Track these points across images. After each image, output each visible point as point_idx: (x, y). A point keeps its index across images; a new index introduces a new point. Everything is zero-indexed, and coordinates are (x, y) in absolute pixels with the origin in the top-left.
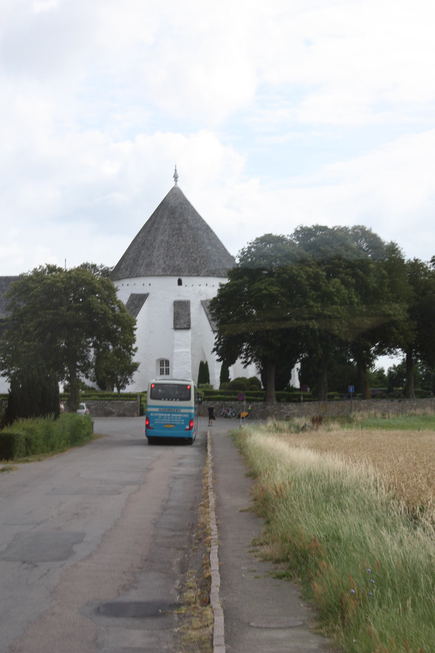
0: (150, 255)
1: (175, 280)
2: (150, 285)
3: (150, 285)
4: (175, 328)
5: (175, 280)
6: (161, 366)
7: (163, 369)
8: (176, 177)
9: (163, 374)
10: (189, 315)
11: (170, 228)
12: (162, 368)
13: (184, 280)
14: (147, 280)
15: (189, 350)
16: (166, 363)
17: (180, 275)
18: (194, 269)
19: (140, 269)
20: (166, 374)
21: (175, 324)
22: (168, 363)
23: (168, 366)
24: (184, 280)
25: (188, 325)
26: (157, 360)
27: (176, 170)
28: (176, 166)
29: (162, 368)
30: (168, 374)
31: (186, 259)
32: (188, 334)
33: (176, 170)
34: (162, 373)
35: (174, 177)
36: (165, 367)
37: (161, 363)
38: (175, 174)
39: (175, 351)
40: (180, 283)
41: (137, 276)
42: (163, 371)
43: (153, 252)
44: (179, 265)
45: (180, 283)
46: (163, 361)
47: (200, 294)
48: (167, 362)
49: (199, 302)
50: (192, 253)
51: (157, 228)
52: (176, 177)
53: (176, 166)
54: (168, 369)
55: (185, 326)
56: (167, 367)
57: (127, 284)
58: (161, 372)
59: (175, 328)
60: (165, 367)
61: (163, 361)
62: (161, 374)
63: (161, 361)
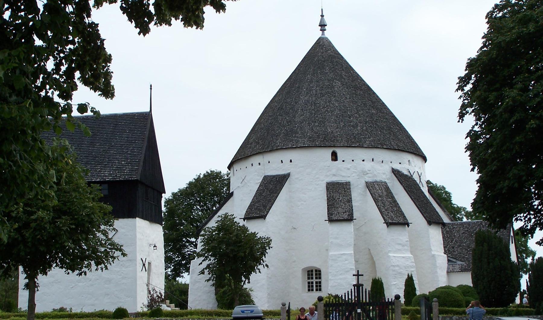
0: (290, 121)
1: (328, 153)
2: (291, 161)
3: (291, 161)
4: (331, 220)
5: (328, 153)
6: (309, 278)
7: (312, 283)
8: (323, 26)
9: (313, 290)
10: (350, 201)
11: (317, 87)
12: (310, 281)
13: (341, 153)
14: (286, 155)
15: (353, 252)
16: (316, 274)
17: (334, 146)
18: (355, 137)
19: (277, 140)
20: (317, 290)
21: (330, 214)
22: (320, 274)
23: (320, 278)
24: (341, 153)
25: (349, 215)
26: (303, 270)
27: (322, 16)
28: (322, 9)
29: (310, 281)
30: (320, 290)
31: (342, 124)
32: (347, 229)
33: (322, 16)
34: (310, 289)
36: (314, 281)
37: (308, 275)
39: (330, 253)
40: (334, 157)
41: (271, 151)
42: (312, 286)
43: (294, 117)
44: (332, 132)
45: (334, 157)
46: (312, 271)
47: (365, 173)
48: (318, 273)
49: (364, 184)
50: (350, 118)
51: (299, 87)
52: (323, 26)
53: (322, 9)
54: (320, 282)
55: (346, 217)
56: (318, 280)
57: (258, 164)
58: (309, 286)
59: (331, 220)
60: (314, 281)
61: (312, 271)
62: (309, 290)
63: (308, 271)
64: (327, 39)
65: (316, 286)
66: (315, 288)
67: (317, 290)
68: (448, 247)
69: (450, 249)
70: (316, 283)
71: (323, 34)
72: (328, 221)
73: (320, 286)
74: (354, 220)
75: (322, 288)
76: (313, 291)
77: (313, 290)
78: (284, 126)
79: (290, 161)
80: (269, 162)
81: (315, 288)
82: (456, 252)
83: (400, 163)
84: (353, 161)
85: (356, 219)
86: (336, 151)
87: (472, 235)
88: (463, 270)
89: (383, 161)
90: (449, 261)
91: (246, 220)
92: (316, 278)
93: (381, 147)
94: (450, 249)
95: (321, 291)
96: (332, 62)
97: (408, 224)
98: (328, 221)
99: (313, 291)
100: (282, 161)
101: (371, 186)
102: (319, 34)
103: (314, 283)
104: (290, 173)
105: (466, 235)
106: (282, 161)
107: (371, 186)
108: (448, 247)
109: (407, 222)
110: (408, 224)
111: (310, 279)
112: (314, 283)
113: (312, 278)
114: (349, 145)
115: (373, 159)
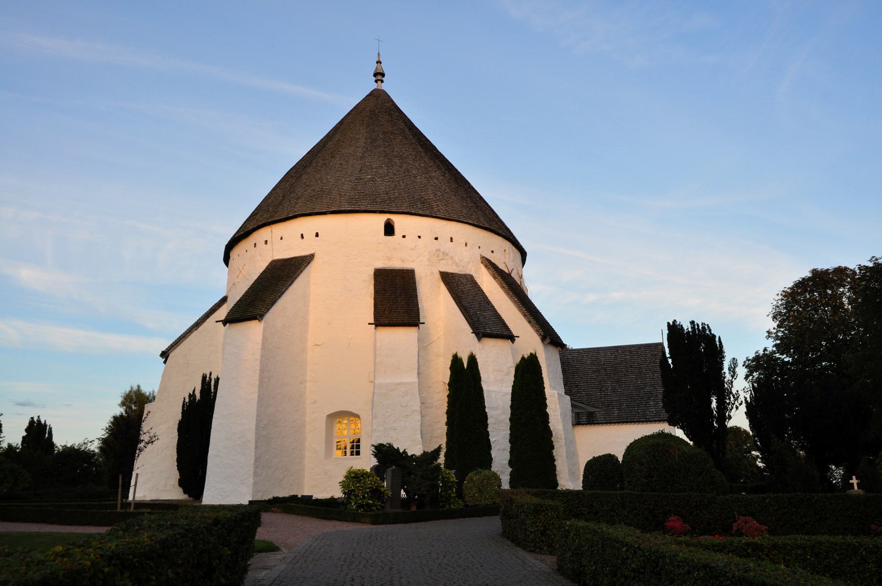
2: (317, 235)
3: (317, 235)
8: (379, 75)
13: (399, 221)
18: (423, 203)
19: (297, 203)
20: (352, 454)
28: (379, 54)
30: (358, 453)
35: (375, 75)
38: (377, 68)
40: (389, 229)
45: (389, 229)
52: (379, 75)
53: (379, 54)
57: (264, 242)
67: (352, 454)
68: (568, 385)
69: (572, 389)
72: (374, 325)
74: (420, 325)
78: (310, 186)
79: (315, 234)
80: (282, 238)
82: (583, 393)
83: (492, 252)
84: (419, 237)
85: (424, 323)
86: (392, 220)
87: (605, 367)
88: (599, 422)
89: (468, 244)
90: (573, 406)
91: (228, 324)
93: (465, 221)
94: (572, 389)
96: (391, 115)
97: (511, 338)
98: (374, 325)
100: (302, 235)
101: (448, 279)
102: (374, 86)
104: (314, 253)
105: (595, 367)
106: (302, 235)
107: (448, 279)
108: (568, 385)
109: (511, 334)
110: (511, 338)
114: (413, 212)
115: (451, 238)
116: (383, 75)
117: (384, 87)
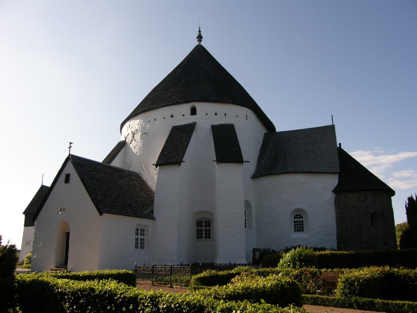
7: (202, 230)
8: (200, 38)
9: (202, 238)
12: (200, 228)
20: (206, 237)
23: (209, 226)
27: (200, 31)
28: (200, 28)
29: (200, 228)
30: (209, 237)
33: (200, 31)
36: (204, 228)
42: (202, 234)
52: (200, 38)
54: (209, 230)
60: (204, 228)
62: (198, 238)
64: (202, 47)
65: (206, 234)
66: (204, 235)
67: (206, 237)
70: (206, 230)
71: (200, 43)
73: (209, 234)
75: (211, 235)
76: (202, 238)
77: (202, 238)
81: (204, 235)
92: (206, 226)
95: (210, 238)
99: (202, 238)
103: (204, 231)
111: (199, 227)
112: (204, 231)
113: (202, 226)
116: (202, 38)
117: (202, 44)
